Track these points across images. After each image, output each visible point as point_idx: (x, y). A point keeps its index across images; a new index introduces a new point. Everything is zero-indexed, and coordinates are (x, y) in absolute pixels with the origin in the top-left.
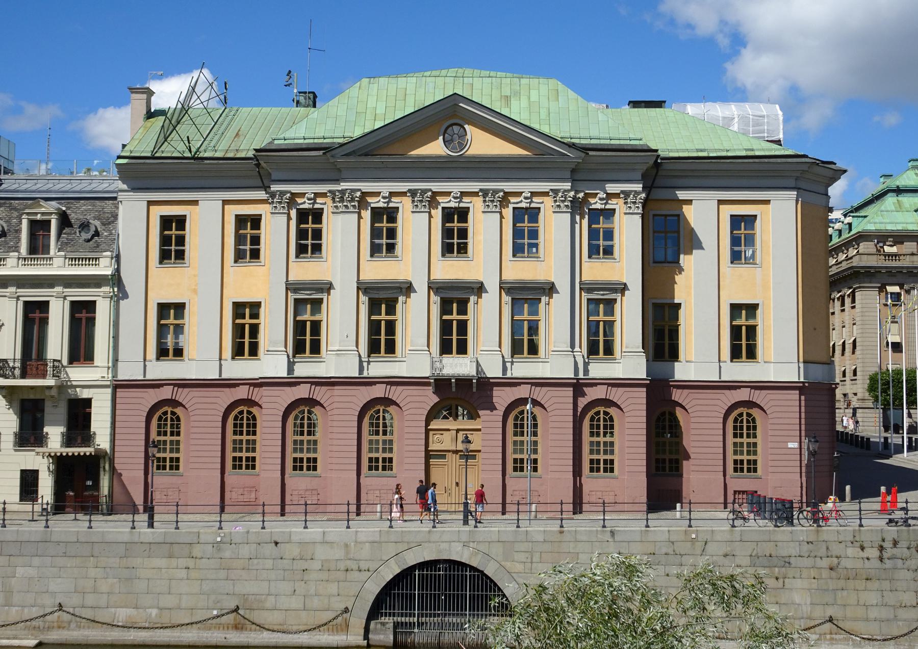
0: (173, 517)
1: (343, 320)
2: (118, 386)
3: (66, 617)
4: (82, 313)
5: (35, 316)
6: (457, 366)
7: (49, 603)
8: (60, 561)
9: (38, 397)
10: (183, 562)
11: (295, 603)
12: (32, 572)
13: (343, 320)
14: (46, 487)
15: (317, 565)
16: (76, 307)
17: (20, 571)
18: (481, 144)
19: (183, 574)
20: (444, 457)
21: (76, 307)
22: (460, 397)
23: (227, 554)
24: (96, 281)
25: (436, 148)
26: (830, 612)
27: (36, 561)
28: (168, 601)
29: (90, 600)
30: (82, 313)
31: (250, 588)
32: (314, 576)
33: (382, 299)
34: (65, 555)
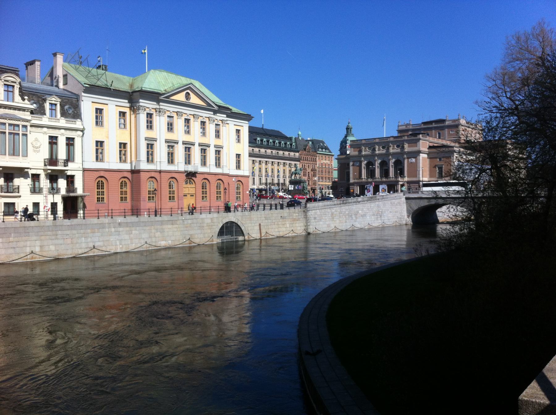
1: (161, 151)
2: (84, 170)
4: (70, 142)
5: (53, 141)
6: (190, 168)
7: (143, 242)
8: (145, 228)
9: (56, 174)
10: (175, 226)
11: (202, 236)
12: (137, 232)
13: (161, 151)
14: (60, 208)
15: (205, 225)
16: (68, 139)
17: (133, 232)
18: (194, 100)
19: (176, 230)
20: (186, 196)
21: (68, 139)
22: (191, 175)
23: (186, 223)
24: (76, 130)
26: (292, 228)
27: (138, 228)
28: (173, 238)
29: (154, 240)
30: (70, 142)
31: (192, 232)
32: (205, 228)
33: (171, 144)
34: (145, 226)
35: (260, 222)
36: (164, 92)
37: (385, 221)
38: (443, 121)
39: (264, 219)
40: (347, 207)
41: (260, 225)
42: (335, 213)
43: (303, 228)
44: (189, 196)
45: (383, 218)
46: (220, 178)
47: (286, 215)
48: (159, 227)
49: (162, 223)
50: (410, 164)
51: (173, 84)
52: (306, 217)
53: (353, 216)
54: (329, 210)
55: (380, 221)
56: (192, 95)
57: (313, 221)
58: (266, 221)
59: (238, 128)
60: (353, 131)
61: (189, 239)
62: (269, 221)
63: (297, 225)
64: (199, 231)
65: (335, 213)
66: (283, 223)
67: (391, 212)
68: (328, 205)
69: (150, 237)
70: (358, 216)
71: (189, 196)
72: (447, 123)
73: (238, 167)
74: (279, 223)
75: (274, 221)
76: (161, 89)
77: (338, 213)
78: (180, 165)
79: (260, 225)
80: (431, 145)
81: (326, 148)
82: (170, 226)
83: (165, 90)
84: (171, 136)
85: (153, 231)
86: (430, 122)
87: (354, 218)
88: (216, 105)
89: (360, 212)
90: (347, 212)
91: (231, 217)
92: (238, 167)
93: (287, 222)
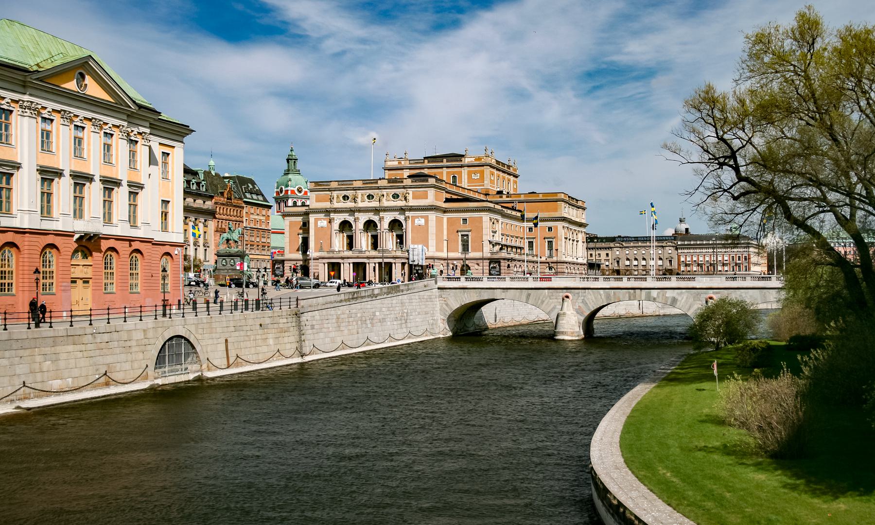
0: (107, 317)
3: (27, 390)
7: (18, 383)
11: (127, 366)
18: (93, 89)
19: (80, 355)
20: (75, 282)
25: (72, 85)
26: (278, 347)
28: (76, 372)
29: (39, 377)
31: (109, 359)
32: (134, 349)
34: (22, 348)
35: (227, 335)
36: (35, 68)
37: (412, 330)
38: (458, 157)
39: (233, 329)
40: (358, 306)
41: (226, 341)
42: (342, 316)
43: (295, 345)
44: (80, 282)
45: (409, 325)
46: (136, 247)
47: (267, 321)
48: (48, 350)
49: (55, 341)
50: (417, 229)
51: (50, 53)
52: (299, 326)
53: (368, 322)
54: (332, 311)
55: (405, 330)
56: (88, 79)
57: (310, 331)
58: (237, 334)
59: (167, 150)
60: (299, 166)
61: (105, 374)
62: (242, 333)
63: (286, 340)
64: (123, 357)
65: (342, 316)
66: (264, 337)
67: (419, 314)
68: (331, 303)
69: (32, 372)
70: (374, 321)
71: (80, 282)
72: (467, 161)
73: (165, 228)
74: (258, 337)
75: (249, 333)
76: (30, 62)
77: (346, 316)
78: (63, 220)
79: (226, 341)
80: (449, 196)
81: (259, 193)
82: (70, 348)
83: (38, 65)
84: (48, 161)
85: (39, 359)
86: (440, 158)
87: (369, 325)
88: (134, 102)
89: (377, 314)
90: (359, 315)
91: (178, 325)
92: (165, 228)
93: (270, 336)
